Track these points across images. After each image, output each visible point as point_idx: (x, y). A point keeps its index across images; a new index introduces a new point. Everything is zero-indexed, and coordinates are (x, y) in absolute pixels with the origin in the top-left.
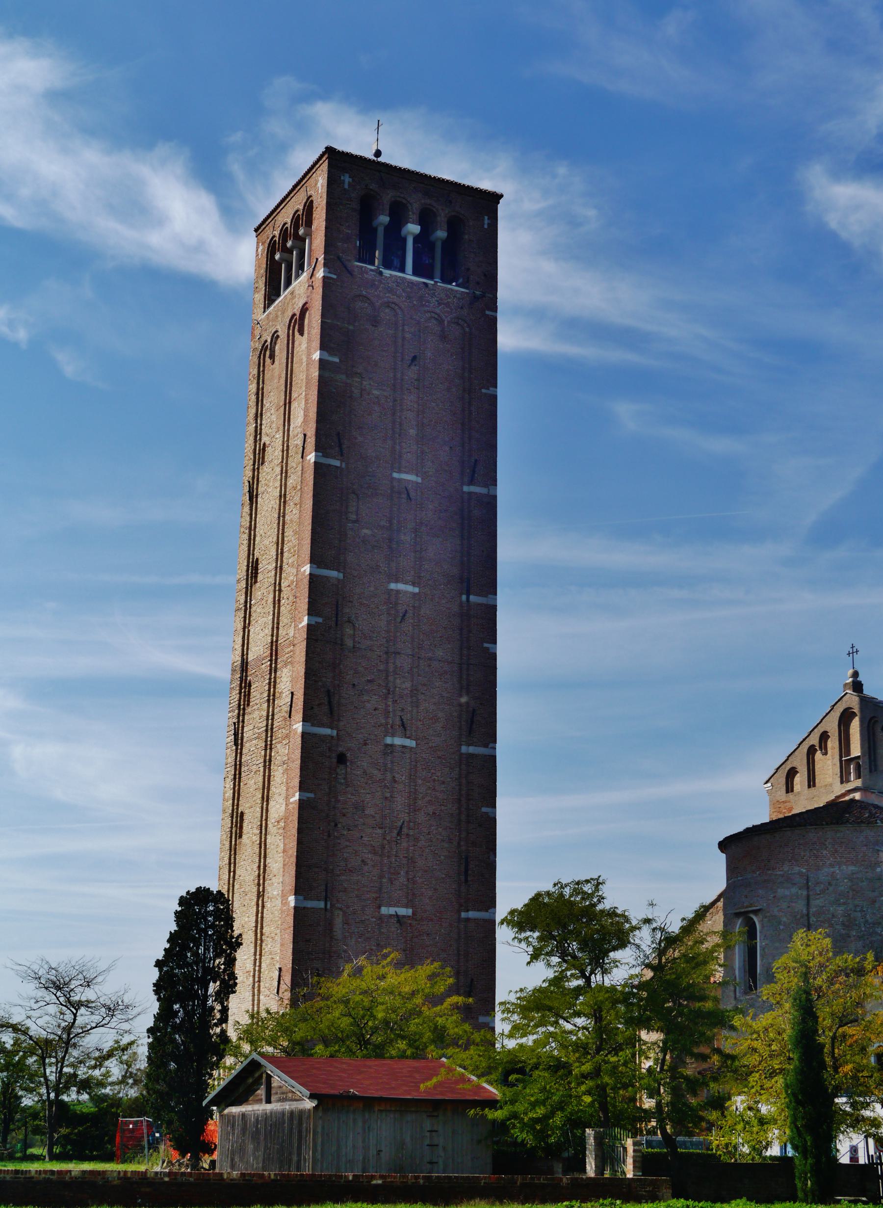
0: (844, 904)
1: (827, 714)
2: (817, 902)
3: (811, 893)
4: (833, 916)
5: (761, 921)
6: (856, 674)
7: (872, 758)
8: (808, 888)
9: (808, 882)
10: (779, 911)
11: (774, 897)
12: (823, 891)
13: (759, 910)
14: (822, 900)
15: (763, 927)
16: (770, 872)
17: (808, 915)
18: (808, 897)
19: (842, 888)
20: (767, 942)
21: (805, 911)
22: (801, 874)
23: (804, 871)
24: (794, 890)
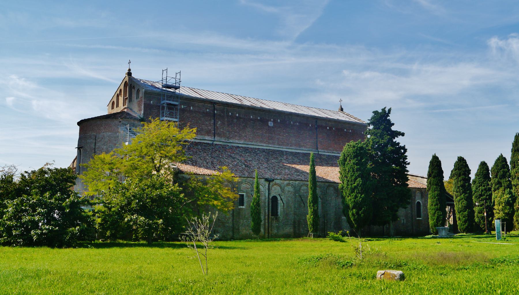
0: (106, 145)
1: (121, 83)
2: (97, 144)
3: (96, 141)
4: (103, 149)
5: (82, 151)
6: (130, 70)
7: (130, 98)
8: (96, 140)
9: (96, 138)
10: (87, 147)
11: (86, 143)
12: (100, 141)
13: (82, 147)
14: (99, 144)
15: (83, 153)
16: (86, 134)
17: (95, 148)
18: (95, 142)
19: (106, 140)
20: (83, 157)
21: (94, 148)
22: (94, 135)
23: (95, 134)
24: (91, 140)
